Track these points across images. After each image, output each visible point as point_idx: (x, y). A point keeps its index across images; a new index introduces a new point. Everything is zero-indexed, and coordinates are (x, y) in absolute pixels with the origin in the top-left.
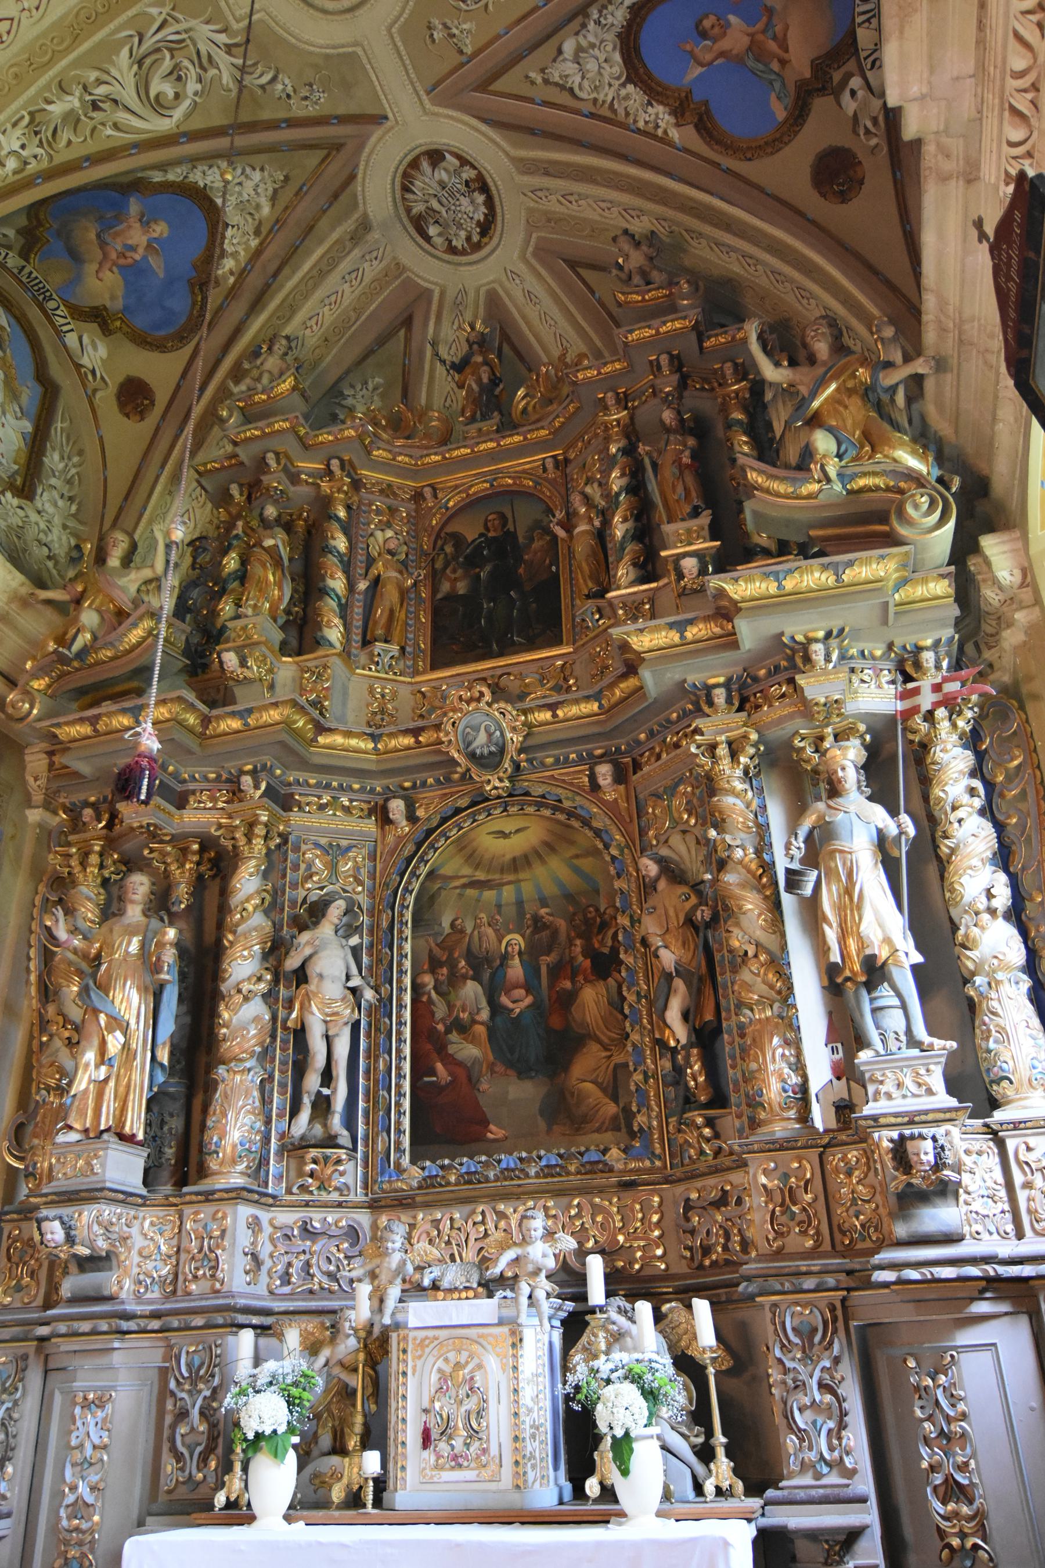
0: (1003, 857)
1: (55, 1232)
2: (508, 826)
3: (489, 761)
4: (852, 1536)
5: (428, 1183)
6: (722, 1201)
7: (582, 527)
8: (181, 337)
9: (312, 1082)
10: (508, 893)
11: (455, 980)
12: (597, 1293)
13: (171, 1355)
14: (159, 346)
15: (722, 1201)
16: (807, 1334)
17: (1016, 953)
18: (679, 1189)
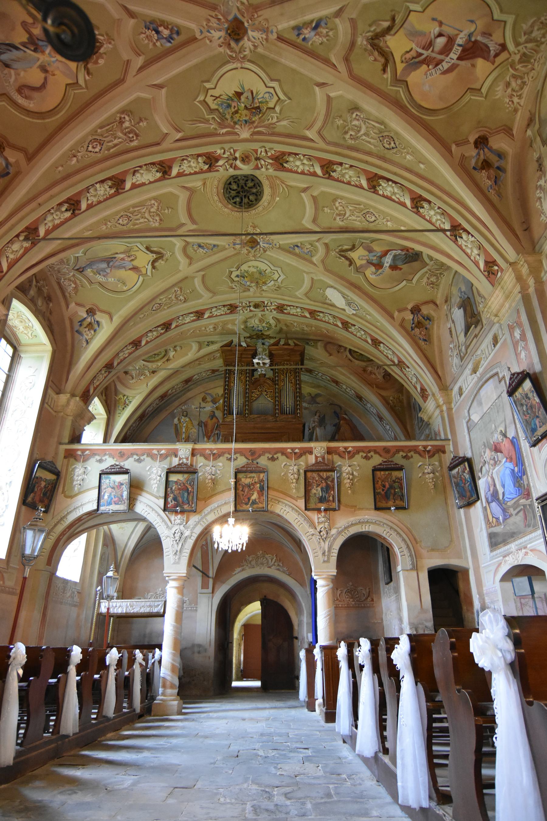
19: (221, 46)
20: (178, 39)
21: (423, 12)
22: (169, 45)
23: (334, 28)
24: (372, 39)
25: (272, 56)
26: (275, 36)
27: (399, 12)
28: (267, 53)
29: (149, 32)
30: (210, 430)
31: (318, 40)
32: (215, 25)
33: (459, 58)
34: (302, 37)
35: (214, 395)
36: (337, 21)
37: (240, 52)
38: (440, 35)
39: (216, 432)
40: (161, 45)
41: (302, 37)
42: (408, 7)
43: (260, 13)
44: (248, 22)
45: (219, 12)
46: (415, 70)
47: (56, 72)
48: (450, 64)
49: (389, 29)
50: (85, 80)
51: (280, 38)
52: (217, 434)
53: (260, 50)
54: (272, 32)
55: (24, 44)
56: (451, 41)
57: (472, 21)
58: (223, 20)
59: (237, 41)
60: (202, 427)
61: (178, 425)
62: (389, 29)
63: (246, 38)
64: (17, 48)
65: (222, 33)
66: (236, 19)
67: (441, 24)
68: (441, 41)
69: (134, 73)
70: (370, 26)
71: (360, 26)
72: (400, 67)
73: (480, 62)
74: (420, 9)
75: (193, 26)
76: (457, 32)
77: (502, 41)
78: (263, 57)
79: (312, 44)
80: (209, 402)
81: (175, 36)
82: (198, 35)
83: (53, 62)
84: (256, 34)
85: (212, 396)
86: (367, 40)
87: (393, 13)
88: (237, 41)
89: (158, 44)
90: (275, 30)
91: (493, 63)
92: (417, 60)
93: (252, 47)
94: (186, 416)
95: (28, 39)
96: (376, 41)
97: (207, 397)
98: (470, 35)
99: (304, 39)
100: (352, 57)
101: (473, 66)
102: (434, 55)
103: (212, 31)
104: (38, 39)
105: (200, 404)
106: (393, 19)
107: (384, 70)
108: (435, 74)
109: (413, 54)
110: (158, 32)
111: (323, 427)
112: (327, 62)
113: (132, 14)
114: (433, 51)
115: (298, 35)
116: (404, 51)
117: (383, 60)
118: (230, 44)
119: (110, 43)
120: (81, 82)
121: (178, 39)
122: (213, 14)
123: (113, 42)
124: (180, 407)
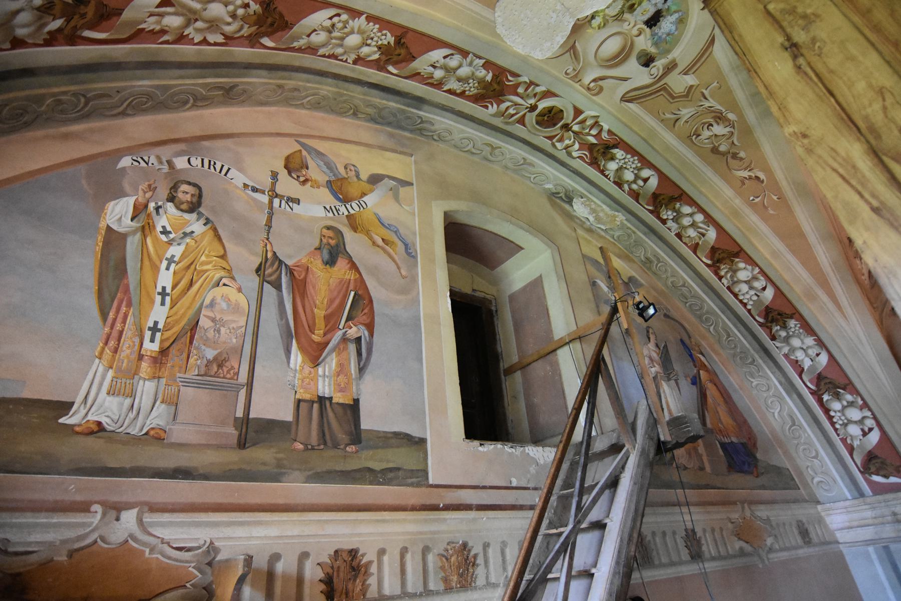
30: (320, 313)
35: (342, 170)
39: (353, 332)
52: (358, 340)
60: (277, 286)
61: (132, 245)
80: (316, 185)
85: (330, 166)
94: (194, 207)
97: (311, 163)
105: (275, 176)
111: (672, 382)
124: (166, 152)
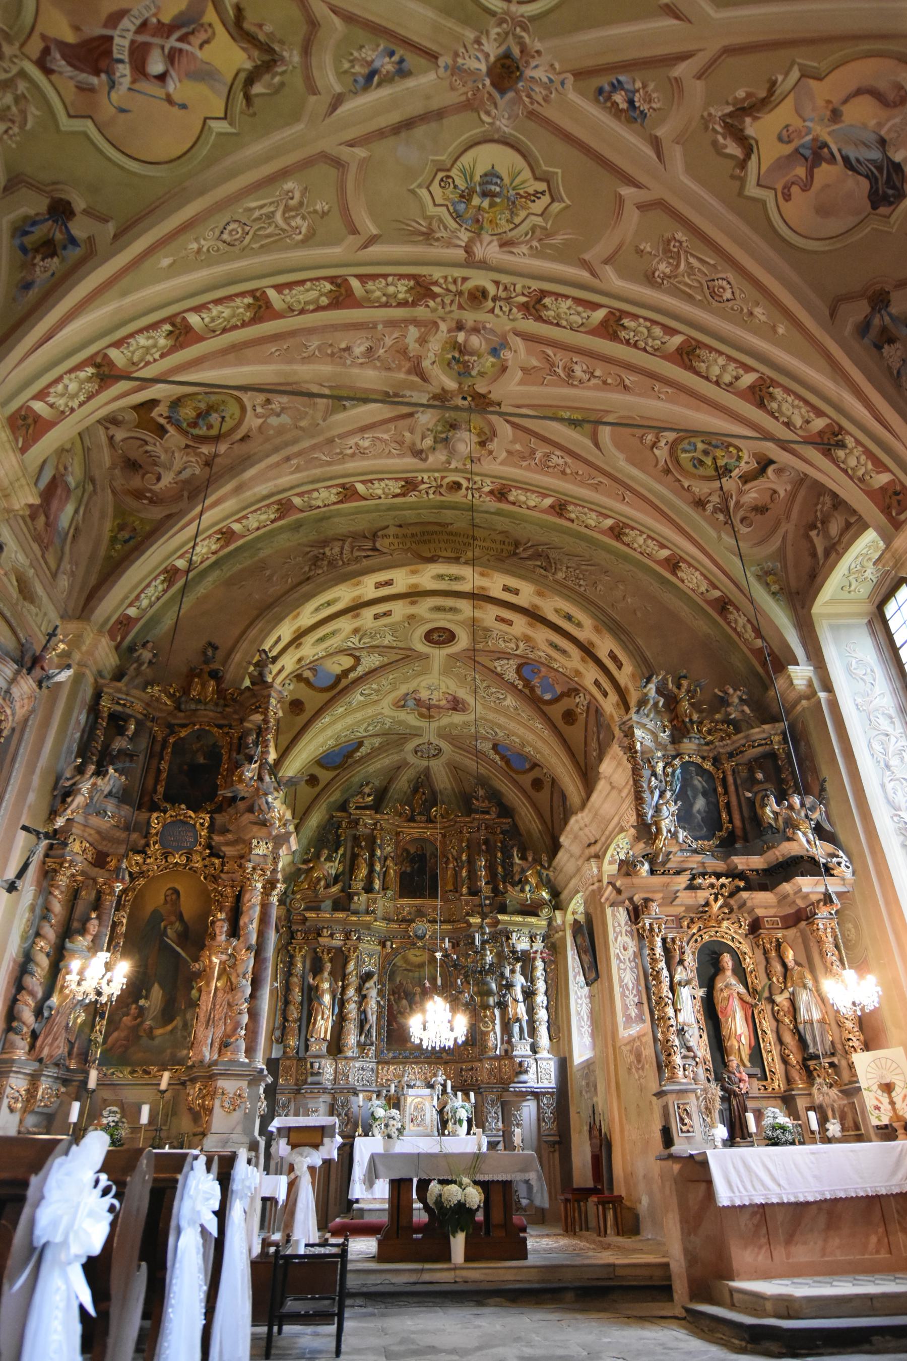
0: (546, 993)
1: (316, 1065)
2: (418, 953)
3: (421, 938)
4: (498, 1142)
5: (394, 1058)
6: (472, 1069)
7: (451, 866)
8: (335, 768)
9: (367, 1027)
10: (417, 974)
11: (400, 998)
12: (449, 1089)
13: (334, 1099)
14: (327, 769)
15: (472, 1069)
16: (493, 1101)
17: (546, 1018)
18: (459, 1065)
19: (538, 52)
20: (604, 82)
21: (206, 119)
22: (622, 78)
23: (341, 74)
24: (275, 61)
25: (449, 23)
26: (441, 62)
27: (242, 112)
28: (459, 29)
29: (645, 107)
31: (368, 54)
32: (537, 89)
33: (110, 39)
34: (396, 58)
36: (338, 88)
37: (507, 34)
38: (162, 78)
40: (634, 81)
41: (396, 58)
42: (231, 124)
43: (463, 98)
44: (484, 85)
45: (525, 106)
46: (182, 13)
47: (820, 103)
48: (121, 26)
49: (250, 80)
50: (786, 74)
51: (433, 57)
53: (470, 35)
54: (446, 67)
55: (832, 159)
56: (139, 68)
57: (122, 111)
58: (523, 94)
59: (507, 55)
62: (250, 80)
63: (492, 59)
64: (846, 160)
65: (529, 73)
66: (502, 91)
67: (169, 100)
68: (156, 66)
69: (700, 54)
70: (282, 84)
71: (298, 82)
72: (211, 16)
73: (70, 38)
74: (212, 124)
75: (573, 96)
76: (137, 86)
77: (54, 77)
78: (466, 22)
79: (378, 46)
81: (607, 88)
82: (570, 79)
83: (812, 120)
84: (473, 64)
86: (282, 59)
87: (251, 111)
88: (507, 55)
89: (638, 85)
90: (441, 71)
91: (44, 37)
92: (184, 30)
93: (484, 40)
95: (820, 165)
96: (267, 58)
98: (112, 85)
99: (392, 54)
100: (304, 29)
101: (77, 29)
102: (156, 40)
103: (545, 80)
104: (806, 159)
106: (248, 98)
107: (239, 9)
108: (141, 9)
109: (197, 40)
110: (631, 102)
112: (349, 18)
113: (656, 144)
114: (163, 48)
115: (402, 61)
116: (213, 43)
117: (246, 26)
118: (522, 52)
119: (710, 115)
120: (795, 74)
121: (604, 82)
122: (536, 106)
123: (705, 114)
